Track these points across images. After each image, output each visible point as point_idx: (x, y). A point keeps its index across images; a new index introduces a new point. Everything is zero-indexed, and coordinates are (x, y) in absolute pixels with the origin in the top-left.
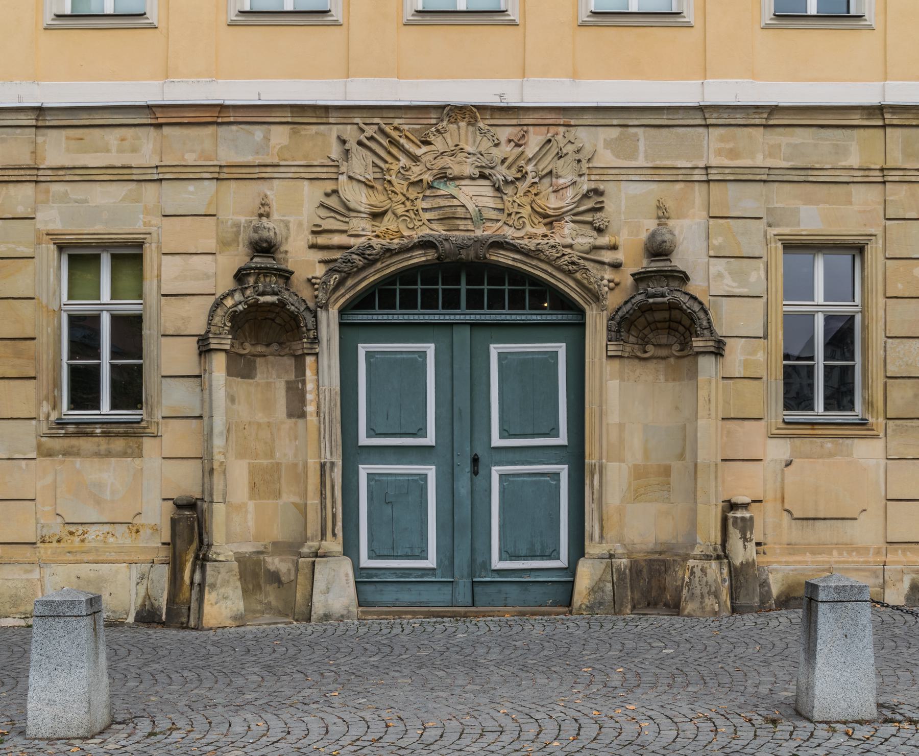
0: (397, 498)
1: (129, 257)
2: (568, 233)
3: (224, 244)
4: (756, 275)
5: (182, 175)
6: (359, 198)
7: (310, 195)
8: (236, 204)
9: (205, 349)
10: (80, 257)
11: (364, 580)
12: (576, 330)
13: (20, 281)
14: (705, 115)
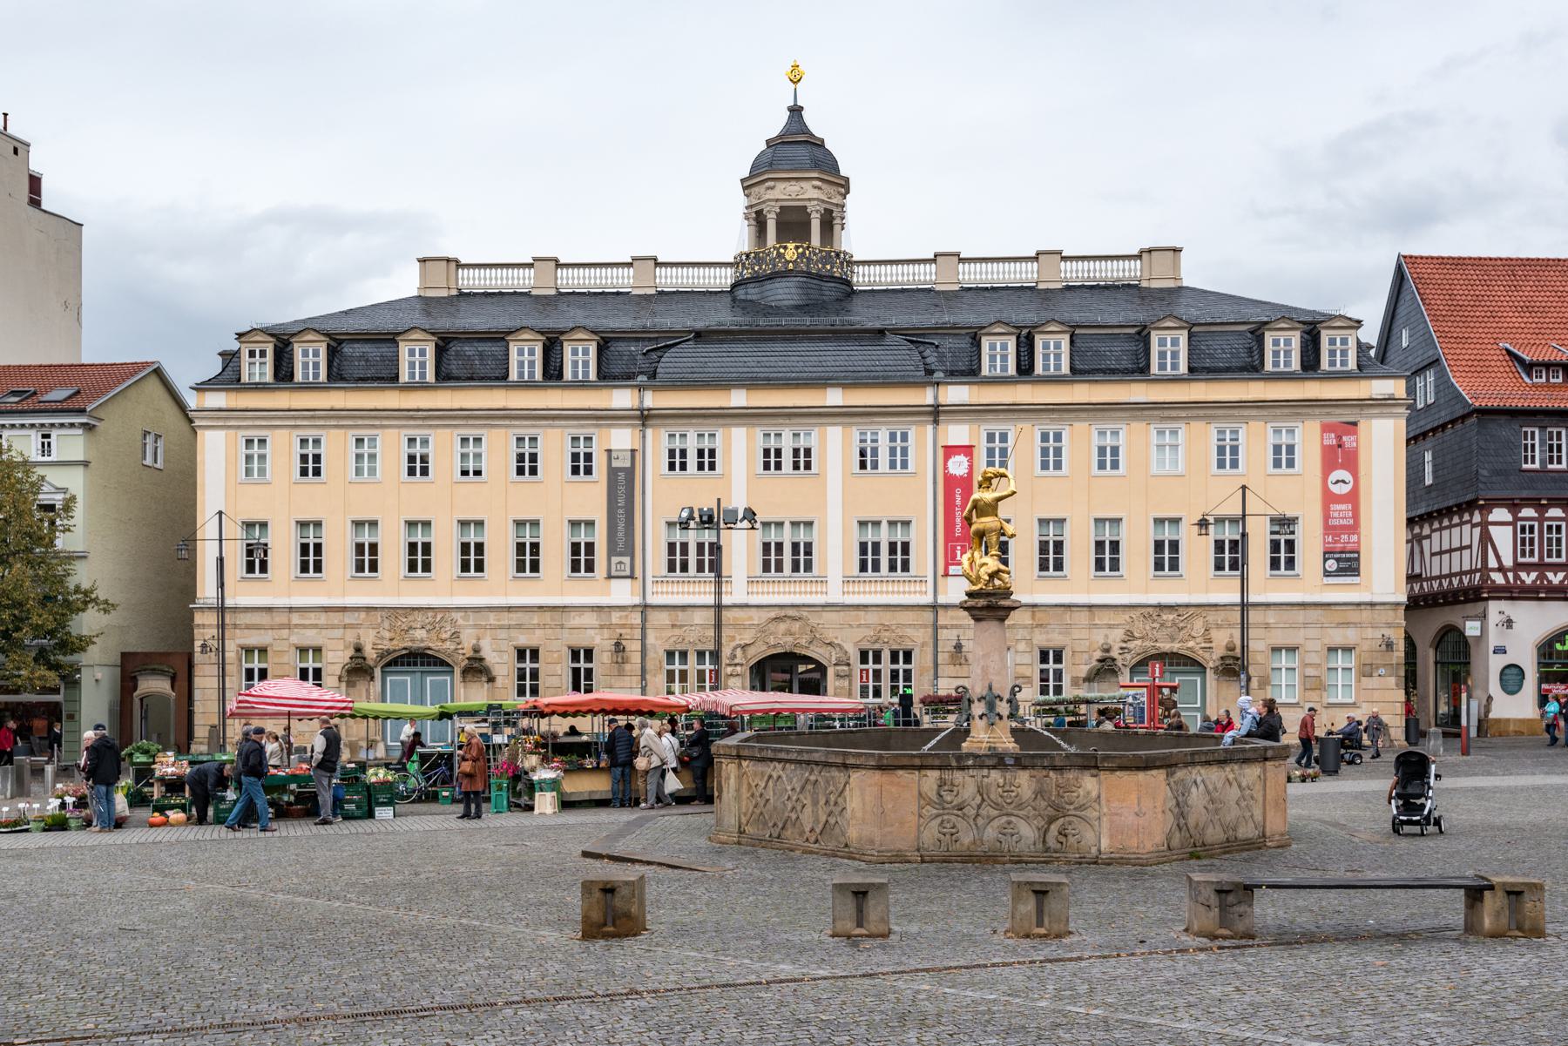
1: (318, 650)
3: (346, 647)
4: (505, 657)
5: (333, 627)
6: (387, 635)
7: (372, 633)
8: (350, 636)
9: (340, 678)
13: (285, 659)
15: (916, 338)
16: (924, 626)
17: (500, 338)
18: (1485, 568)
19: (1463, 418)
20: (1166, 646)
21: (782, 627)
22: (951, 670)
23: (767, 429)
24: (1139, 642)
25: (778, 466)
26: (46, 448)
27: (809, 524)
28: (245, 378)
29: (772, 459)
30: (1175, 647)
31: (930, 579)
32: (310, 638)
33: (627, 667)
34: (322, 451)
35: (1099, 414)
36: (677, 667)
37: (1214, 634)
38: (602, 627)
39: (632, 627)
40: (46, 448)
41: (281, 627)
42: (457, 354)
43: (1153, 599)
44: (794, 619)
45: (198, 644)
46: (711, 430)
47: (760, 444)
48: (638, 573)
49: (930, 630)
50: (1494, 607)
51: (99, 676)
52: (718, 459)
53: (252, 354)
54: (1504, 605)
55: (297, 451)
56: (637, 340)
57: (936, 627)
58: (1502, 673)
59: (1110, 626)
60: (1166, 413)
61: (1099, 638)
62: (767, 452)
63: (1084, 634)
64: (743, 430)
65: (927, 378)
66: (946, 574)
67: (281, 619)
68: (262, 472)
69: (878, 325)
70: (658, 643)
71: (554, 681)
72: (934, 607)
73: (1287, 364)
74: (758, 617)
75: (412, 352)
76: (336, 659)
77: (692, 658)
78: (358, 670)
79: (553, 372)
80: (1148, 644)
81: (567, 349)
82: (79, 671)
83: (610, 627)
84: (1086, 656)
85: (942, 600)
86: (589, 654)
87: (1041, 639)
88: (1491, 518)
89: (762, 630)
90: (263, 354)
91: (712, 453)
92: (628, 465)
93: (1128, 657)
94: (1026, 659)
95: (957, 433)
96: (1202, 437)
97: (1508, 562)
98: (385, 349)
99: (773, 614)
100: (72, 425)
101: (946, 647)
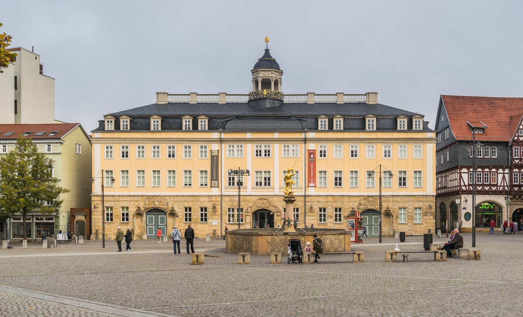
0: (151, 229)
1: (127, 208)
2: (165, 206)
4: (182, 210)
5: (132, 201)
7: (143, 203)
8: (136, 204)
10: (123, 208)
11: (148, 236)
12: (166, 215)
13: (118, 210)
14: (177, 196)
15: (300, 119)
16: (302, 201)
17: (180, 117)
18: (460, 186)
19: (455, 143)
20: (370, 207)
21: (261, 201)
22: (310, 214)
23: (257, 145)
24: (362, 206)
25: (260, 155)
26: (49, 149)
27: (269, 172)
28: (106, 129)
29: (258, 153)
30: (373, 207)
31: (304, 188)
32: (125, 204)
33: (217, 213)
34: (129, 150)
35: (352, 141)
36: (231, 213)
38: (209, 201)
39: (218, 201)
40: (49, 149)
41: (117, 201)
42: (168, 122)
43: (366, 194)
44: (265, 199)
45: (93, 206)
46: (241, 145)
47: (255, 149)
48: (220, 186)
49: (304, 202)
50: (463, 196)
51: (64, 215)
52: (271, 153)
53: (108, 122)
54: (465, 196)
55: (121, 150)
56: (220, 118)
57: (305, 202)
58: (465, 215)
59: (354, 202)
60: (370, 141)
61: (351, 205)
62: (257, 151)
64: (250, 145)
65: (302, 130)
66: (309, 187)
67: (116, 199)
68: (111, 156)
69: (289, 115)
70: (225, 206)
71: (195, 217)
72: (305, 196)
73: (404, 128)
74: (254, 199)
75: (154, 122)
76: (132, 210)
77: (236, 210)
78: (139, 214)
79: (195, 128)
81: (199, 121)
82: (59, 213)
83: (211, 201)
85: (307, 194)
86: (206, 209)
87: (335, 205)
88: (462, 171)
89: (255, 202)
90: (111, 122)
91: (269, 151)
92: (217, 154)
94: (331, 211)
95: (311, 146)
96: (381, 148)
97: (467, 184)
98: (146, 120)
99: (259, 198)
100: (57, 143)
101: (308, 208)
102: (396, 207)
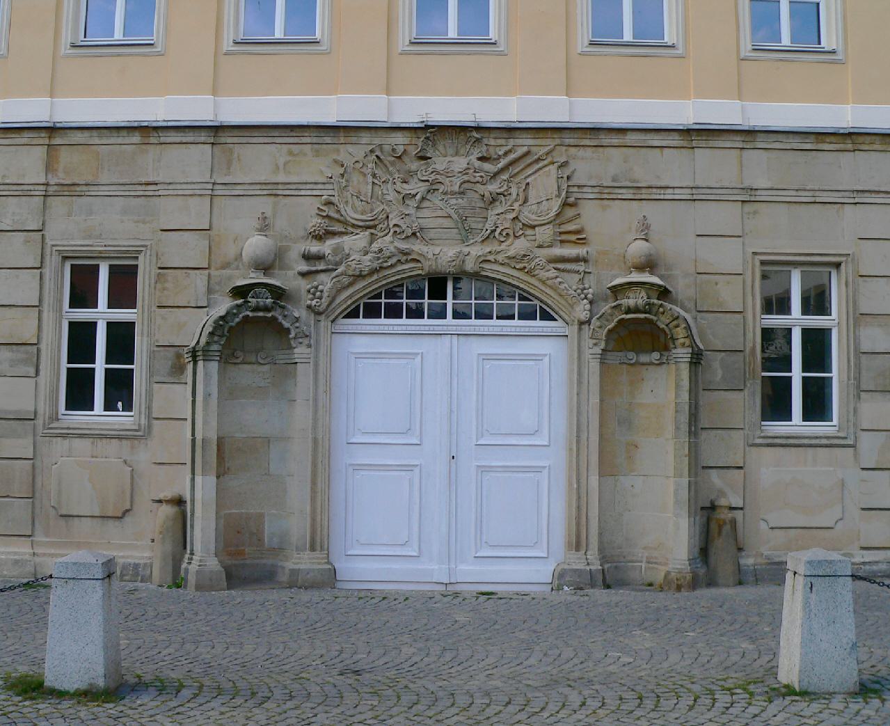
37: (591, 216)
63: (195, 213)
80: (387, 243)
84: (200, 280)
93: (326, 282)
102: (728, 256)
